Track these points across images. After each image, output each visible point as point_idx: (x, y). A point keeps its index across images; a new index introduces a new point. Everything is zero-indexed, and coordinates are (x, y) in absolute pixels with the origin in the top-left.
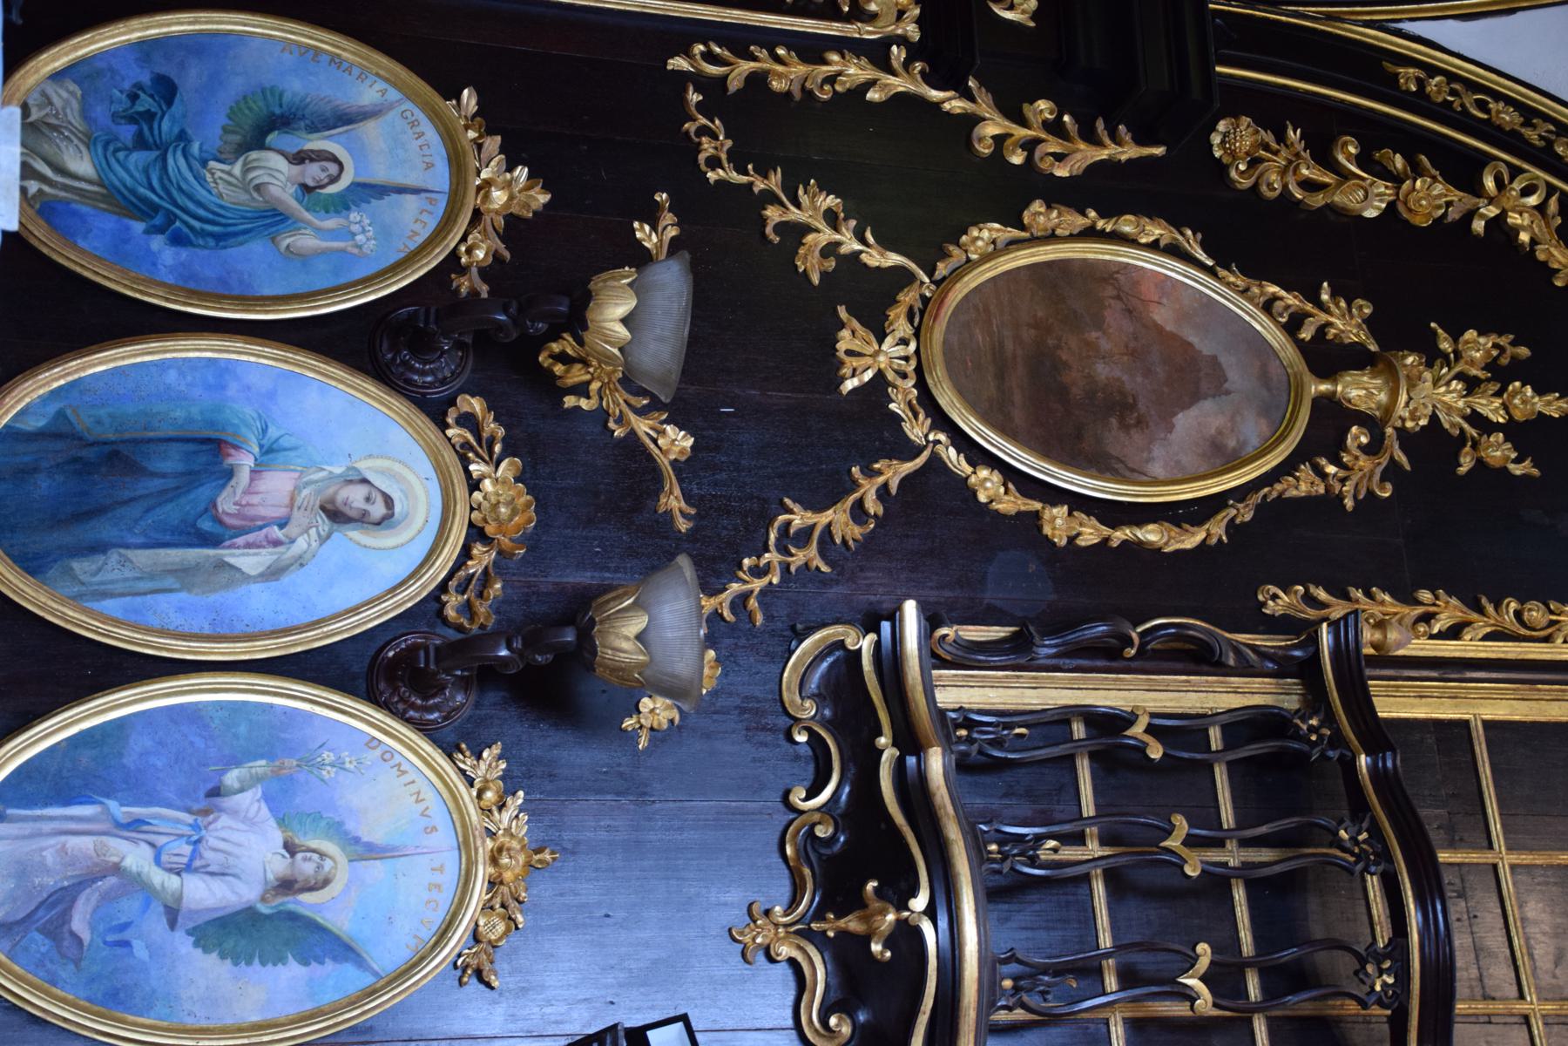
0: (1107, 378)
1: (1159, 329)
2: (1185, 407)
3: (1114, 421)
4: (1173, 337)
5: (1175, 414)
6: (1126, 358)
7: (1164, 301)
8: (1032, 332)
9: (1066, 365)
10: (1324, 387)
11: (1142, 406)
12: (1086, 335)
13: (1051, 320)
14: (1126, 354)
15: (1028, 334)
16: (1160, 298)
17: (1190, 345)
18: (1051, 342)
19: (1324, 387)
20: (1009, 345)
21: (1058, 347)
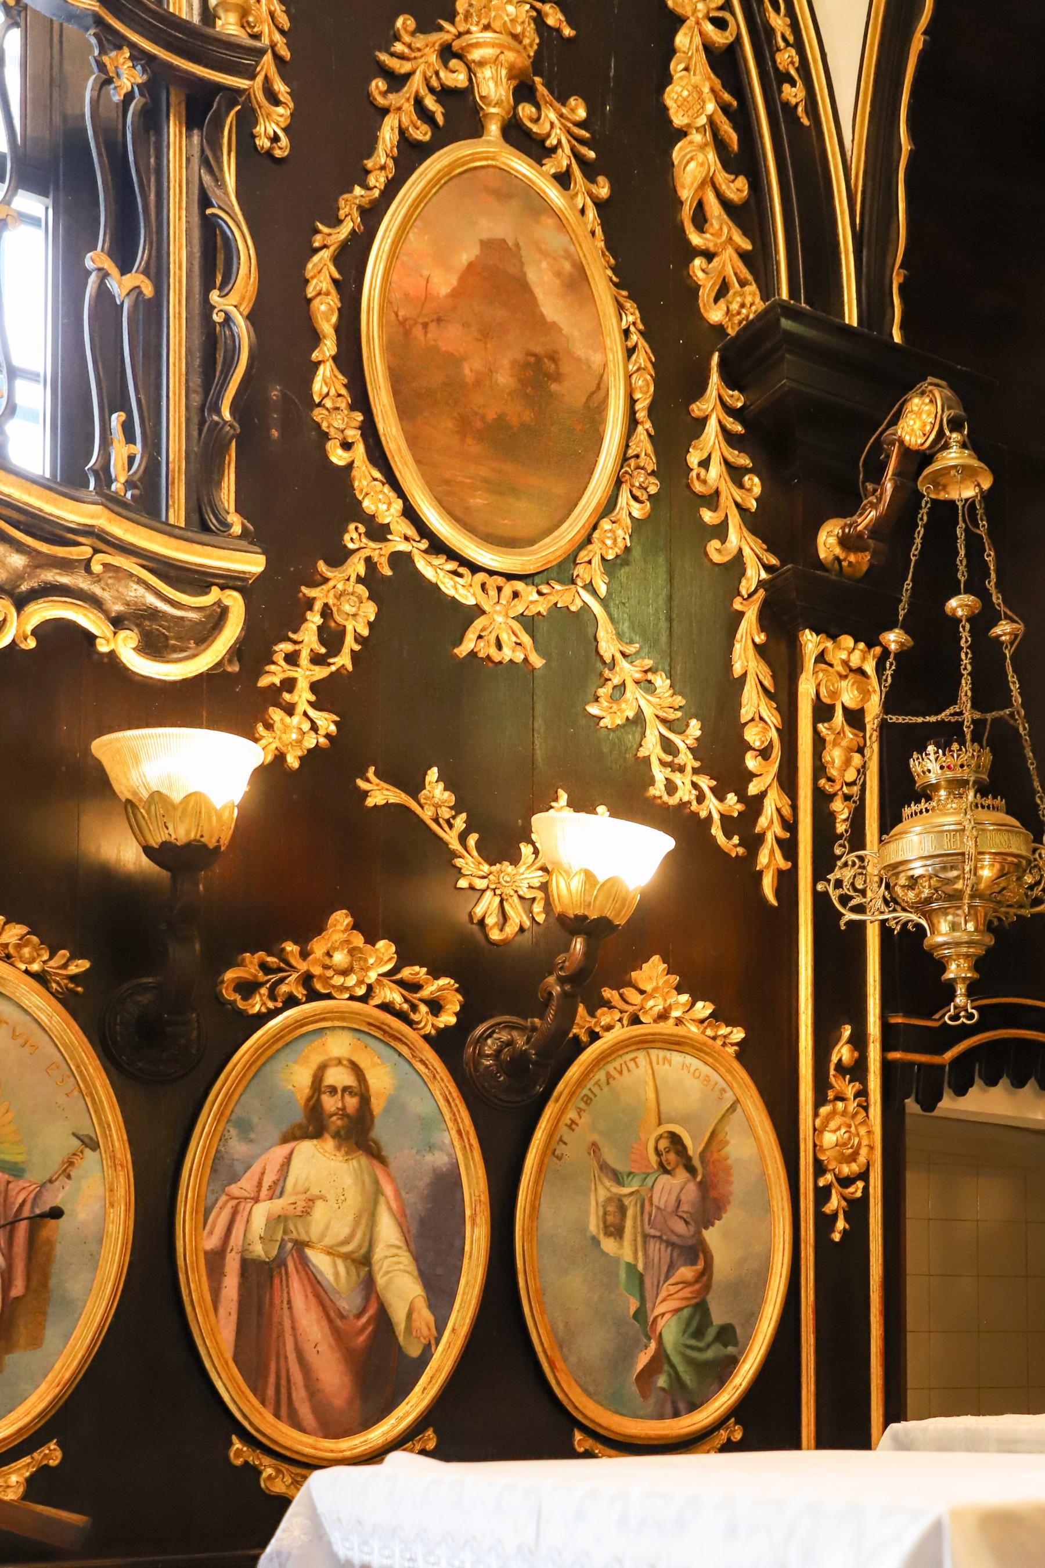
0: (512, 376)
1: (455, 294)
2: (533, 301)
3: (554, 387)
4: (462, 279)
5: (542, 315)
6: (489, 346)
7: (426, 273)
8: (469, 440)
9: (501, 418)
10: (494, 129)
11: (538, 349)
12: (467, 380)
13: (455, 415)
14: (486, 343)
15: (473, 447)
16: (421, 276)
17: (470, 265)
18: (479, 424)
19: (494, 129)
20: (484, 472)
21: (483, 417)
